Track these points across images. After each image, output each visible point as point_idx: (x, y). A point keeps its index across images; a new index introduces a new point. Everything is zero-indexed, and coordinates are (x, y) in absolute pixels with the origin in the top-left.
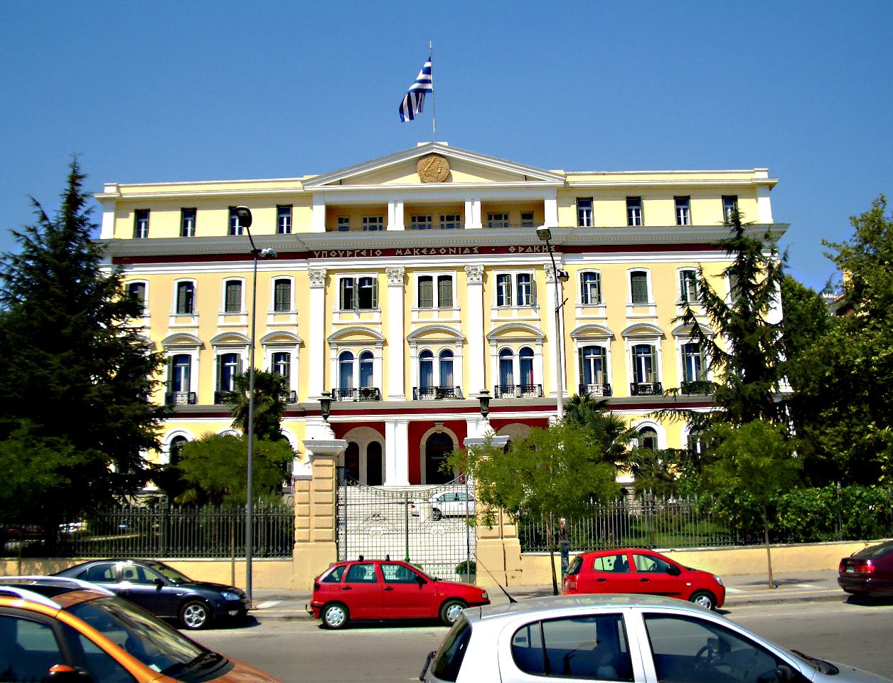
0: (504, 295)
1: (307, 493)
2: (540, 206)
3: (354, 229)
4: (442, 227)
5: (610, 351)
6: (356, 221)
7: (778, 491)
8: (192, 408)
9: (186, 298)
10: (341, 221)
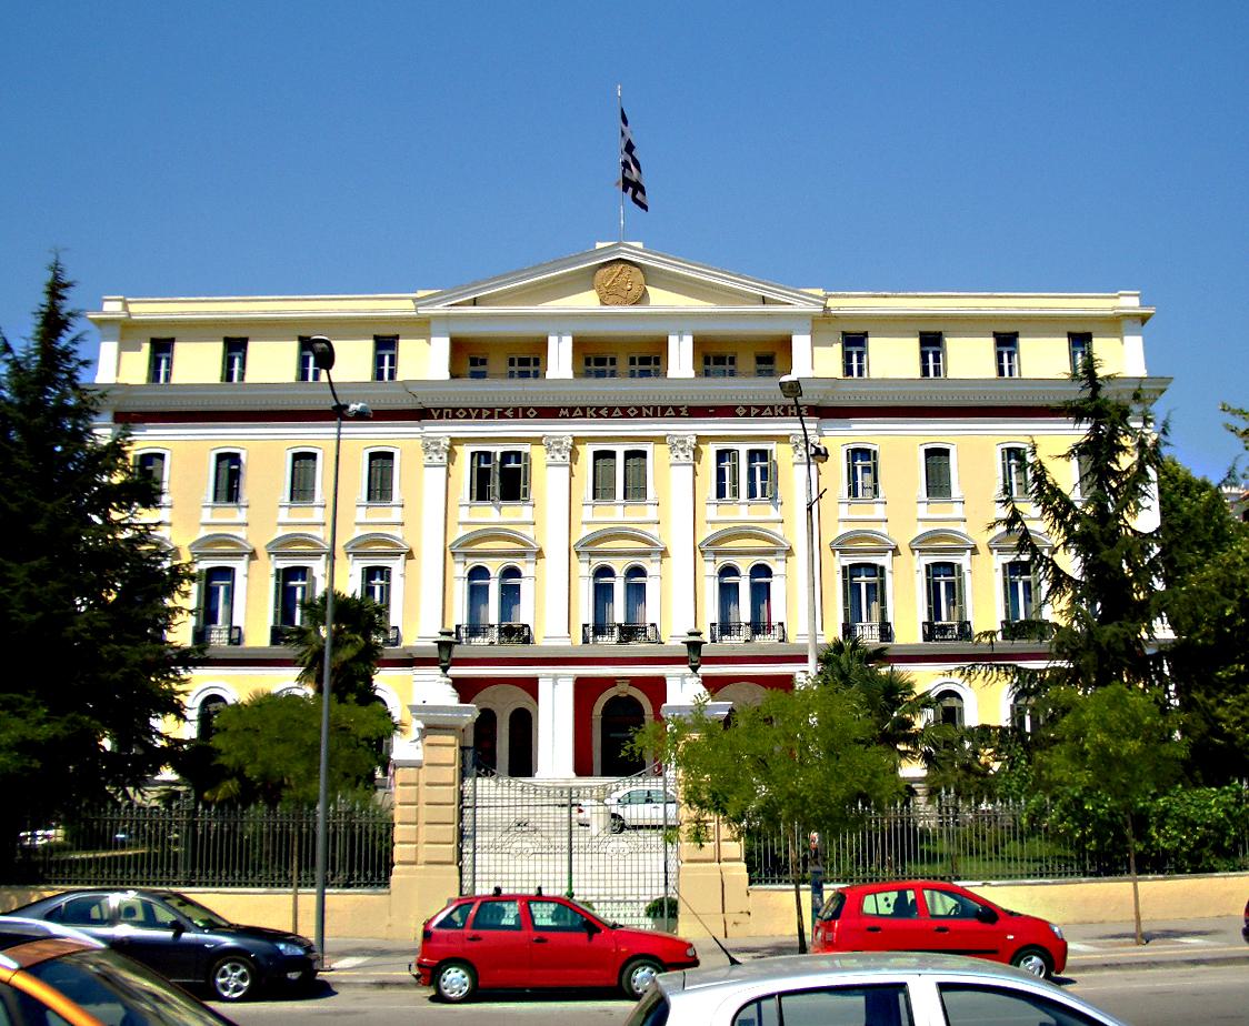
0: (727, 482)
1: (414, 788)
2: (786, 344)
3: (494, 376)
4: (632, 375)
5: (891, 572)
6: (497, 363)
7: (1152, 792)
8: (234, 652)
9: (229, 479)
10: (474, 362)
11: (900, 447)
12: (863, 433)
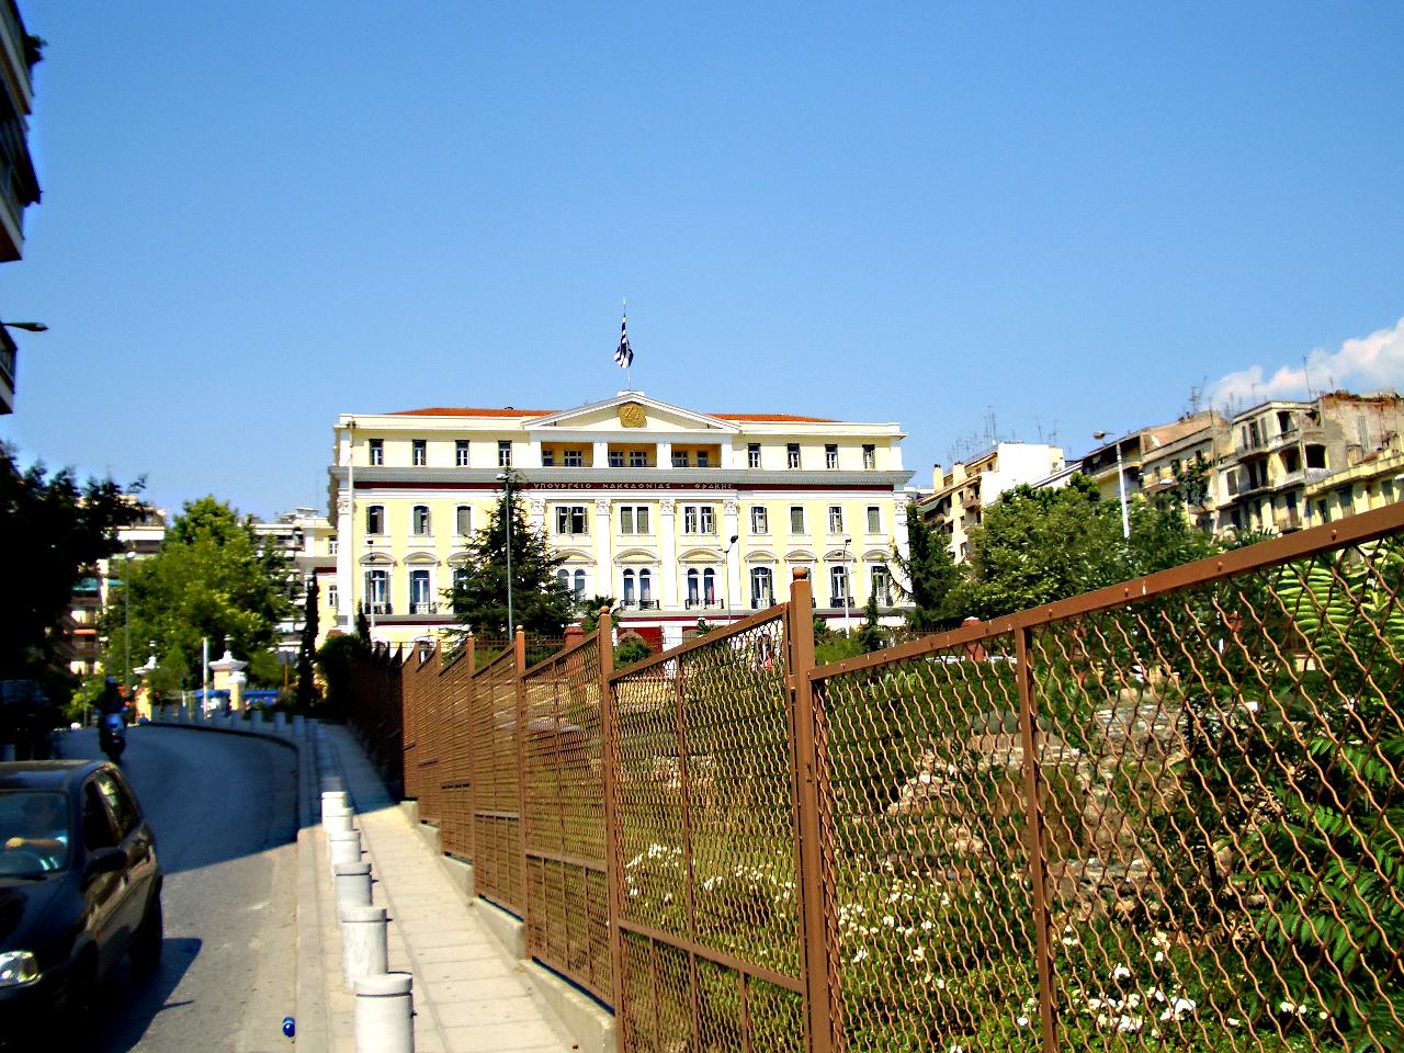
2: (716, 448)
4: (566, 464)
11: (778, 505)
12: (759, 498)
